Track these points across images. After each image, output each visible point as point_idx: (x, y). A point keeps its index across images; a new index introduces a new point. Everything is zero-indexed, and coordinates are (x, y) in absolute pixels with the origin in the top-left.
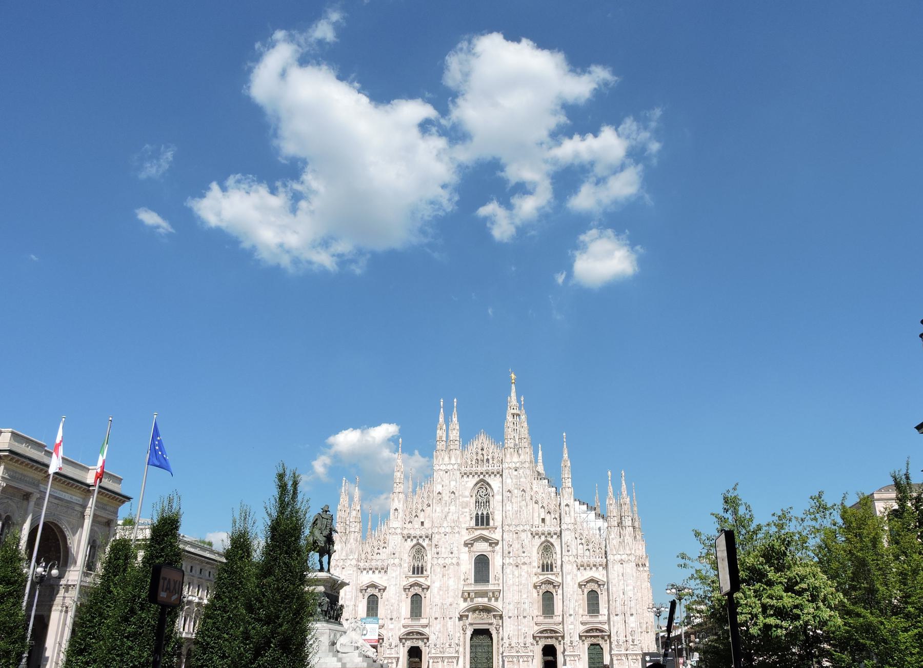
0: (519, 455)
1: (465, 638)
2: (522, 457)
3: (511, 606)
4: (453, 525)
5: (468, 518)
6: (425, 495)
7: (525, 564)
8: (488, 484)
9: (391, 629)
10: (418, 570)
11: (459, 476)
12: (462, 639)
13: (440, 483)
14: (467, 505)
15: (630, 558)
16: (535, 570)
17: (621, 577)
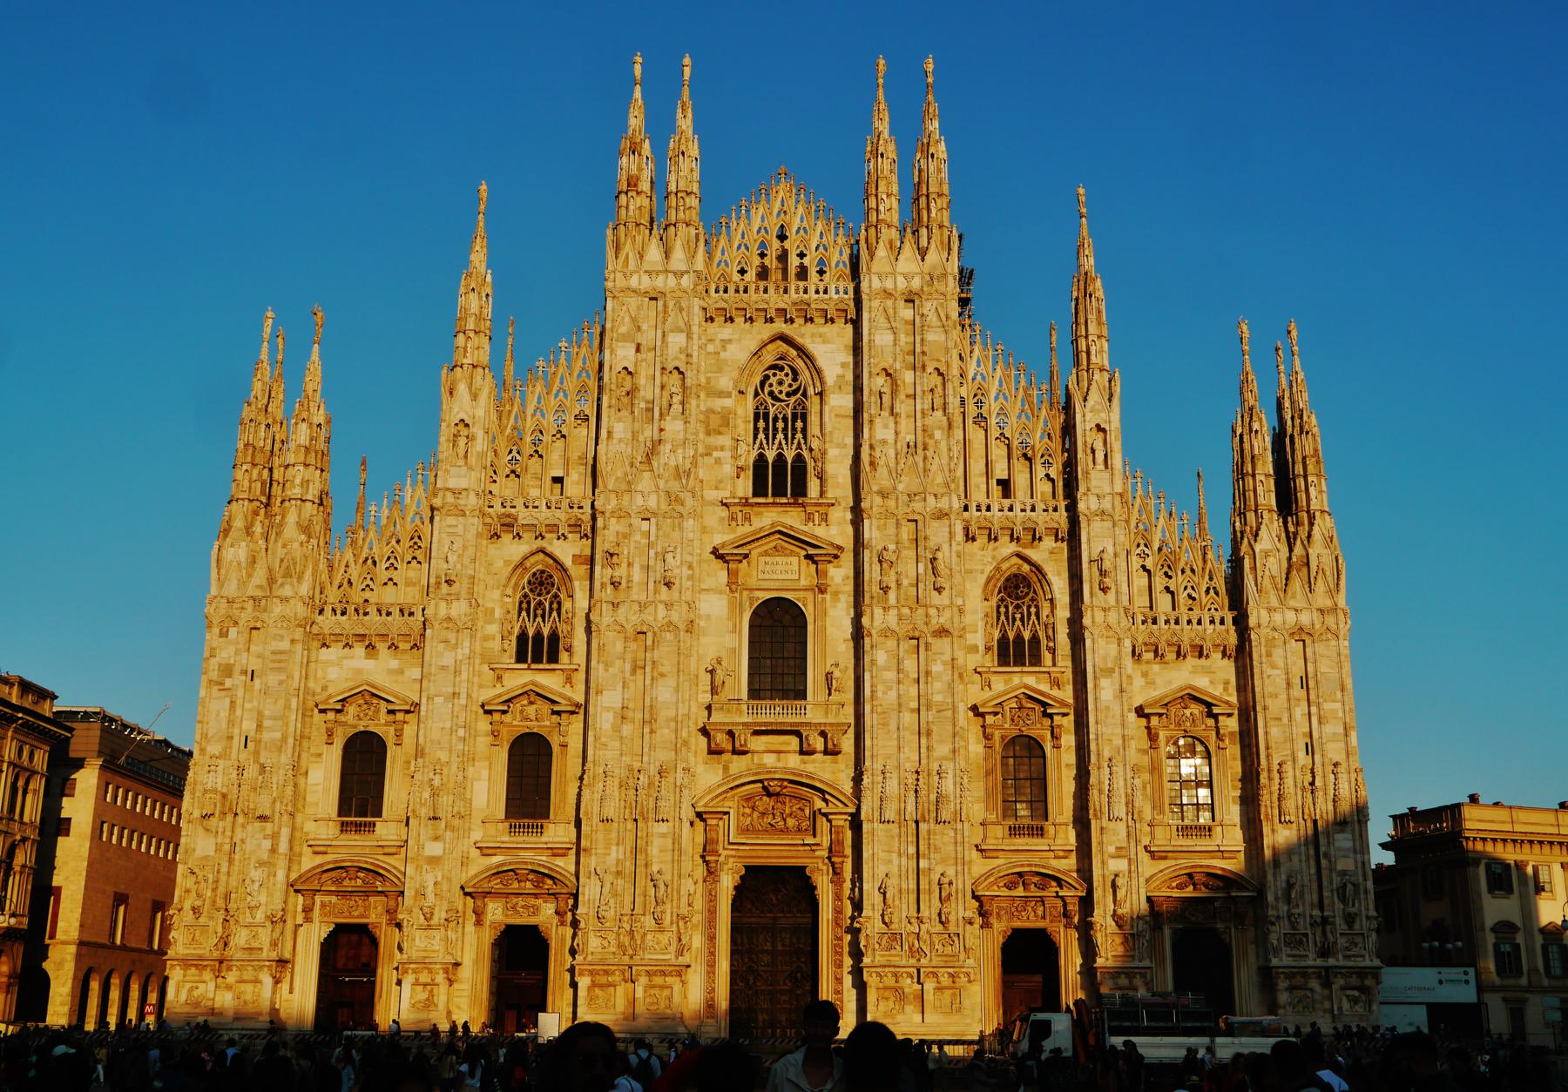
0: (923, 253)
1: (712, 898)
2: (933, 257)
3: (892, 787)
4: (674, 486)
5: (728, 469)
6: (572, 384)
7: (942, 632)
8: (802, 351)
9: (434, 861)
10: (538, 649)
11: (697, 316)
12: (699, 904)
13: (625, 338)
14: (726, 419)
15: (1330, 620)
16: (973, 661)
17: (1298, 692)
